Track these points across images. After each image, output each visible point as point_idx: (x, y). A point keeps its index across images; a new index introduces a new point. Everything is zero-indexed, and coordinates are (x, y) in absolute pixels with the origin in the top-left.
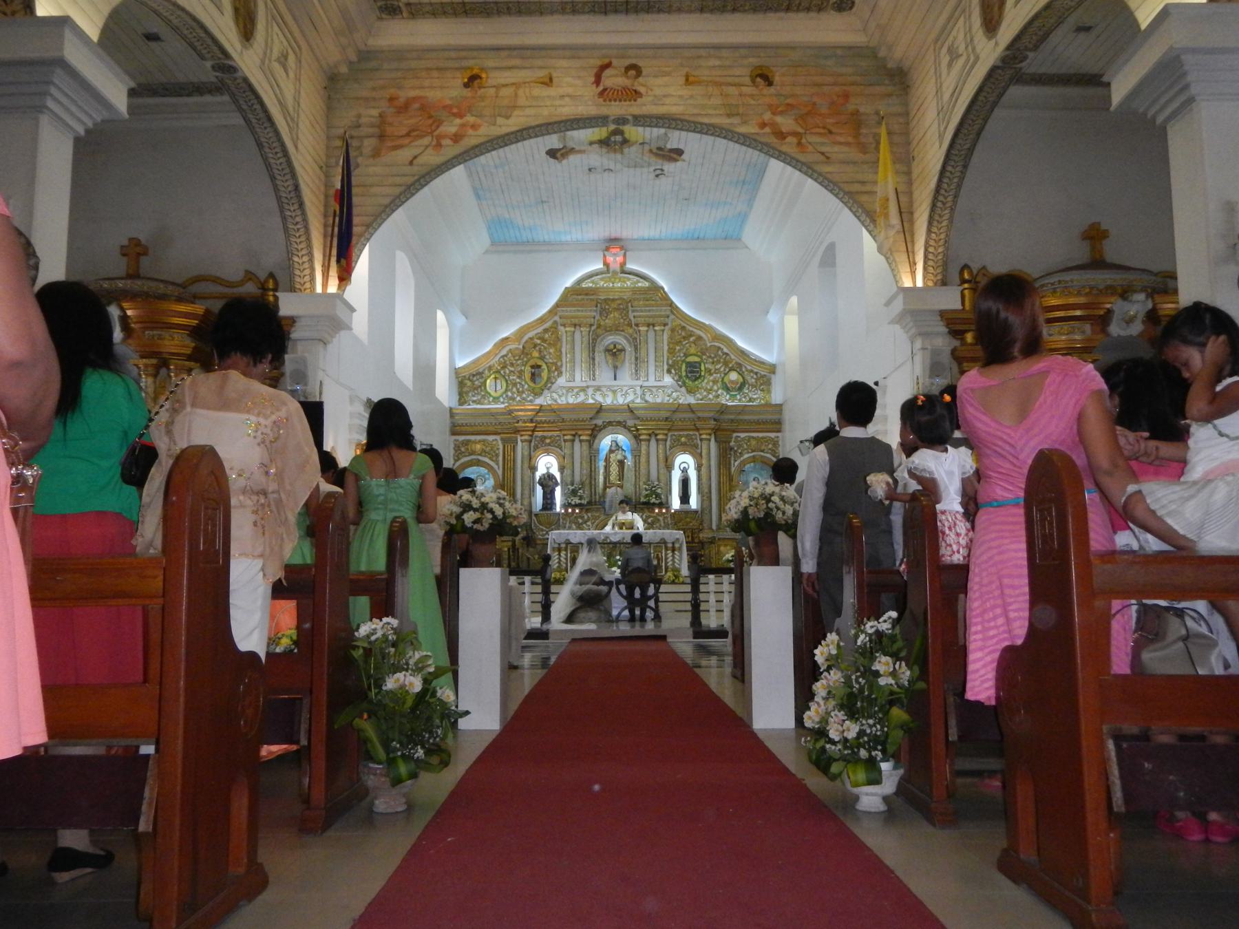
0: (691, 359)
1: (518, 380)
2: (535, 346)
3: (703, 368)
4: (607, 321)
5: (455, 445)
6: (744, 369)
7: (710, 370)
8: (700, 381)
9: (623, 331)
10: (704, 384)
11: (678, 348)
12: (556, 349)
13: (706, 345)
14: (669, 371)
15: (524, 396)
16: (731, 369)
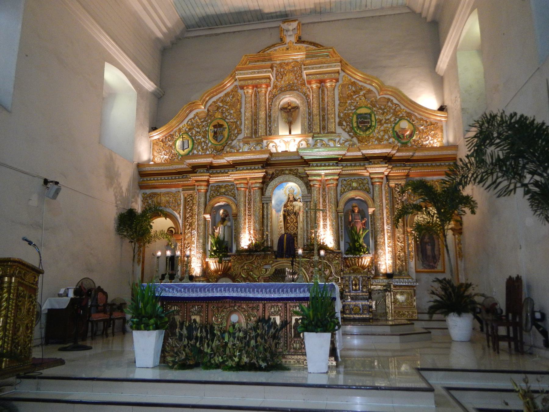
0: (360, 111)
1: (203, 140)
2: (218, 108)
3: (373, 119)
4: (282, 82)
5: (144, 198)
6: (413, 118)
7: (380, 121)
8: (371, 131)
9: (297, 90)
10: (375, 134)
11: (349, 102)
12: (236, 110)
13: (376, 97)
14: (340, 124)
15: (208, 152)
16: (401, 119)
